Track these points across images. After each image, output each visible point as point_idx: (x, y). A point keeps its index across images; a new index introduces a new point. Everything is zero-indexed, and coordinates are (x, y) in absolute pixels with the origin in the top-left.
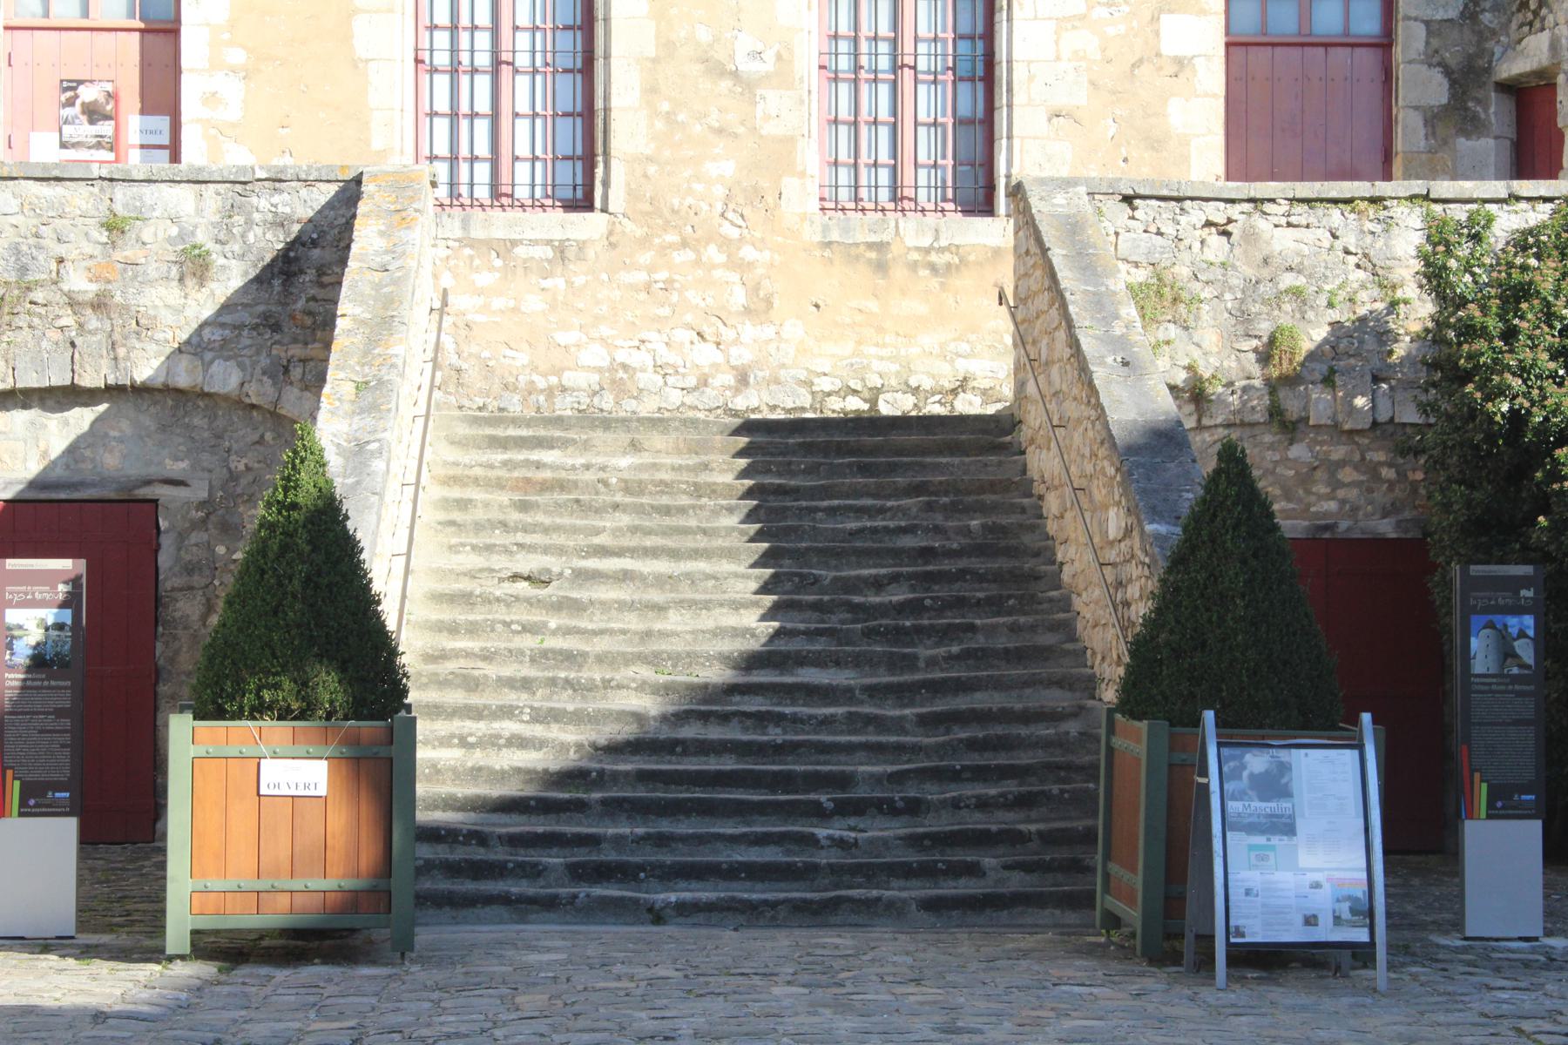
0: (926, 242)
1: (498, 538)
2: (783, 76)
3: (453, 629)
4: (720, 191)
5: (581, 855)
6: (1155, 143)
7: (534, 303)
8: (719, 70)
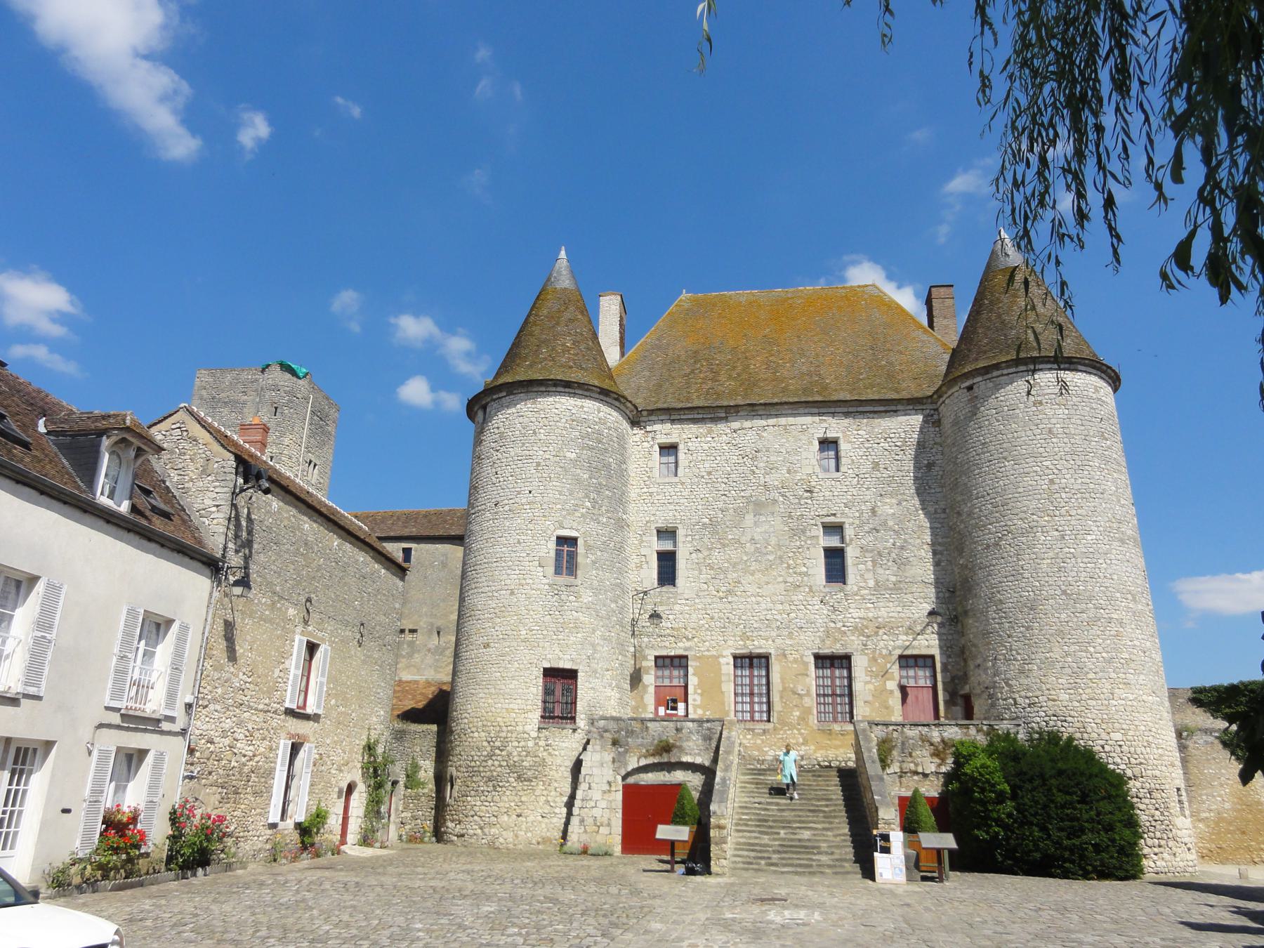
0: (840, 729)
1: (752, 795)
3: (743, 814)
6: (887, 708)
7: (759, 742)
8: (795, 693)
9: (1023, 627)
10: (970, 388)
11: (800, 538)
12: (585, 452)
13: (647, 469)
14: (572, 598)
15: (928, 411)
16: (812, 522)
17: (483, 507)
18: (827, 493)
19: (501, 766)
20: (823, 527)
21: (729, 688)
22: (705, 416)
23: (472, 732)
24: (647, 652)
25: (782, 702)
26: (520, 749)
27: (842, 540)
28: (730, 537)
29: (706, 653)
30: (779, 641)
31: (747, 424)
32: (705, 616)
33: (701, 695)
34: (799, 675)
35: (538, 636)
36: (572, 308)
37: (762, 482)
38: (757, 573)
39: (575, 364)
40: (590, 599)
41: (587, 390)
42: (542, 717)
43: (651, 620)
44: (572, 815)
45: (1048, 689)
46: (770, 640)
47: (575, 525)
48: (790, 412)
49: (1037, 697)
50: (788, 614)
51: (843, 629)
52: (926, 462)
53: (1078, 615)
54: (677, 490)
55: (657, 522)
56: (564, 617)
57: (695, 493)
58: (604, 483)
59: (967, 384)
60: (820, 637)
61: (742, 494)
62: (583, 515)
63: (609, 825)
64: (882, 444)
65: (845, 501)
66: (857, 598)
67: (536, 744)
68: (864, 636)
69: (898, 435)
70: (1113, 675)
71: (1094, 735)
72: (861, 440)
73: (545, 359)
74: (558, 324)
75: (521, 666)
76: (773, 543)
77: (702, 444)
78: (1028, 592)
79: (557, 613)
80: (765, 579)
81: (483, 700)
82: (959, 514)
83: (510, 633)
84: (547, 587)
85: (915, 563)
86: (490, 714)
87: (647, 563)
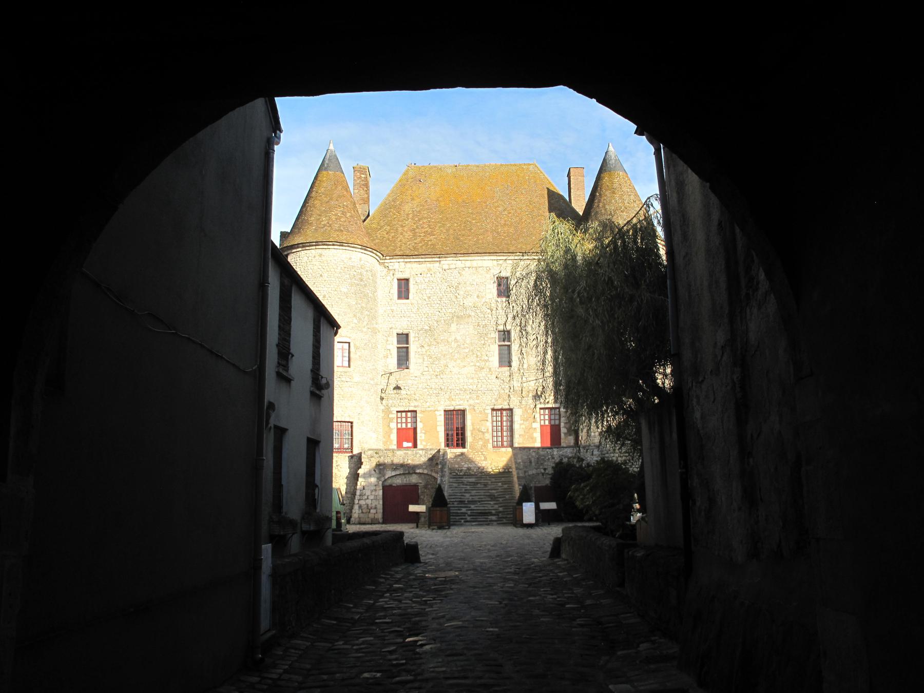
4: (480, 446)
6: (532, 438)
8: (479, 431)
11: (484, 338)
13: (390, 294)
24: (392, 409)
25: (472, 437)
28: (442, 338)
33: (425, 433)
34: (483, 420)
36: (340, 188)
37: (461, 304)
38: (458, 360)
43: (395, 391)
73: (325, 225)
74: (331, 199)
76: (468, 342)
77: (424, 279)
79: (340, 389)
87: (391, 355)
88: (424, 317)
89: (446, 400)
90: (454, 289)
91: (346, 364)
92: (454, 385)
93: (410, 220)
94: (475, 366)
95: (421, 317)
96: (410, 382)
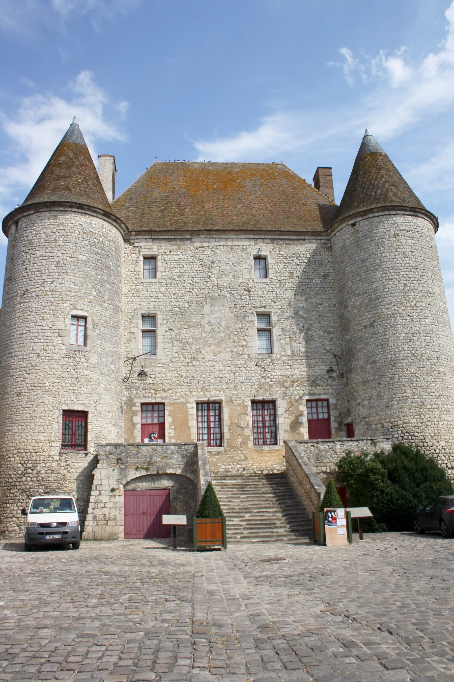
2: (248, 427)
5: (241, 535)
8: (239, 426)
9: (388, 377)
10: (353, 225)
11: (242, 322)
12: (92, 256)
13: (135, 273)
14: (83, 360)
15: (324, 241)
16: (250, 311)
17: (15, 294)
18: (260, 292)
19: (32, 481)
20: (257, 315)
21: (193, 424)
22: (176, 237)
23: (10, 457)
24: (136, 400)
25: (230, 433)
26: (46, 469)
27: (270, 323)
28: (194, 321)
29: (177, 401)
30: (227, 392)
31: (205, 244)
32: (176, 375)
33: (174, 429)
34: (242, 414)
35: (59, 387)
37: (216, 283)
38: (213, 346)
39: (85, 194)
40: (96, 361)
41: (94, 212)
42: (62, 445)
44: (87, 513)
45: (404, 417)
46: (222, 391)
47: (85, 308)
48: (235, 237)
49: (397, 422)
50: (234, 374)
51: (271, 383)
52: (323, 274)
53: (421, 369)
54: (157, 287)
55: (142, 310)
56: (78, 373)
57: (169, 290)
58: (106, 279)
59: (352, 222)
60: (255, 388)
61: (202, 291)
62: (90, 302)
63: (115, 519)
64: (295, 261)
65: (272, 298)
66: (279, 362)
67: (59, 464)
68: (284, 387)
69: (305, 255)
70: (441, 406)
71: (430, 444)
72: (282, 258)
73: (63, 189)
75: (46, 409)
77: (174, 257)
78: (391, 355)
79: (72, 370)
80: (219, 349)
81: (17, 434)
82: (346, 307)
83: (37, 385)
84: (65, 352)
85: (317, 339)
86: (23, 444)
87: (135, 338)
88: (173, 297)
89: (199, 390)
90: (207, 268)
91: (81, 343)
92: (208, 374)
93: (157, 203)
94: (232, 352)
95: (170, 297)
96: (157, 369)
